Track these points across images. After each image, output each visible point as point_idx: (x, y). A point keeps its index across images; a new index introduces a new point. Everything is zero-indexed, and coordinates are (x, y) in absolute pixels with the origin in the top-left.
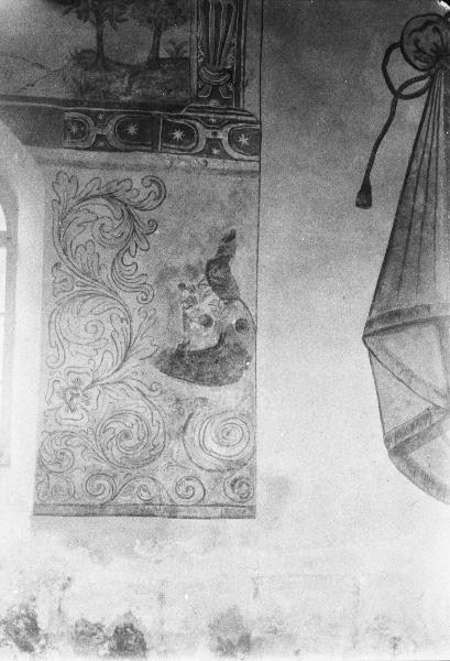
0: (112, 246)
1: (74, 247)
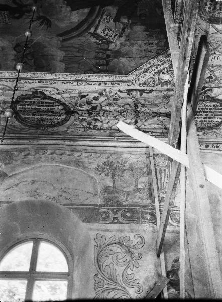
0: (122, 265)
1: (104, 267)
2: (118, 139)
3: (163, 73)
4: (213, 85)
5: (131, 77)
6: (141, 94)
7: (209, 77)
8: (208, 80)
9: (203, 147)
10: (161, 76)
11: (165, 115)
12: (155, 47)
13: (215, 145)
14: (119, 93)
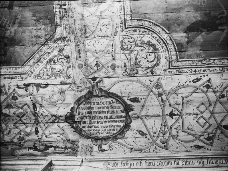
2: (19, 158)
3: (54, 62)
4: (102, 75)
5: (26, 68)
6: (38, 90)
7: (97, 65)
8: (95, 68)
9: (111, 164)
10: (54, 66)
11: (63, 118)
12: (43, 31)
13: (125, 162)
14: (17, 89)
